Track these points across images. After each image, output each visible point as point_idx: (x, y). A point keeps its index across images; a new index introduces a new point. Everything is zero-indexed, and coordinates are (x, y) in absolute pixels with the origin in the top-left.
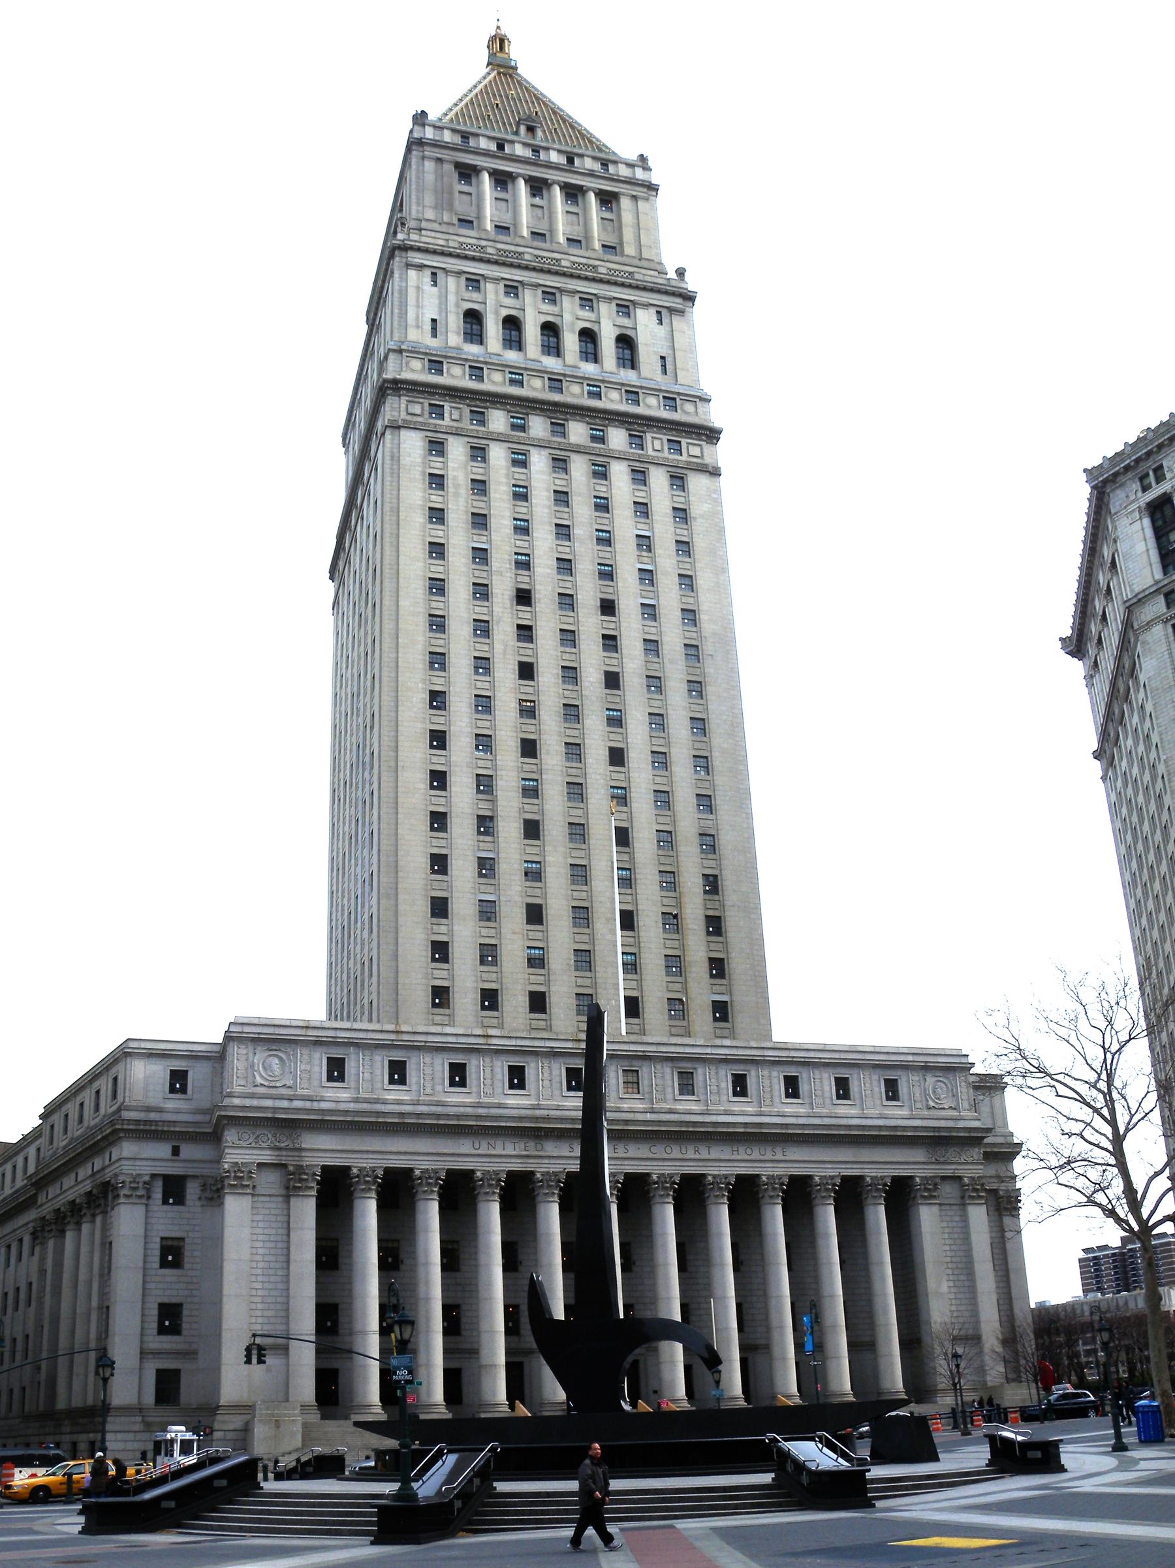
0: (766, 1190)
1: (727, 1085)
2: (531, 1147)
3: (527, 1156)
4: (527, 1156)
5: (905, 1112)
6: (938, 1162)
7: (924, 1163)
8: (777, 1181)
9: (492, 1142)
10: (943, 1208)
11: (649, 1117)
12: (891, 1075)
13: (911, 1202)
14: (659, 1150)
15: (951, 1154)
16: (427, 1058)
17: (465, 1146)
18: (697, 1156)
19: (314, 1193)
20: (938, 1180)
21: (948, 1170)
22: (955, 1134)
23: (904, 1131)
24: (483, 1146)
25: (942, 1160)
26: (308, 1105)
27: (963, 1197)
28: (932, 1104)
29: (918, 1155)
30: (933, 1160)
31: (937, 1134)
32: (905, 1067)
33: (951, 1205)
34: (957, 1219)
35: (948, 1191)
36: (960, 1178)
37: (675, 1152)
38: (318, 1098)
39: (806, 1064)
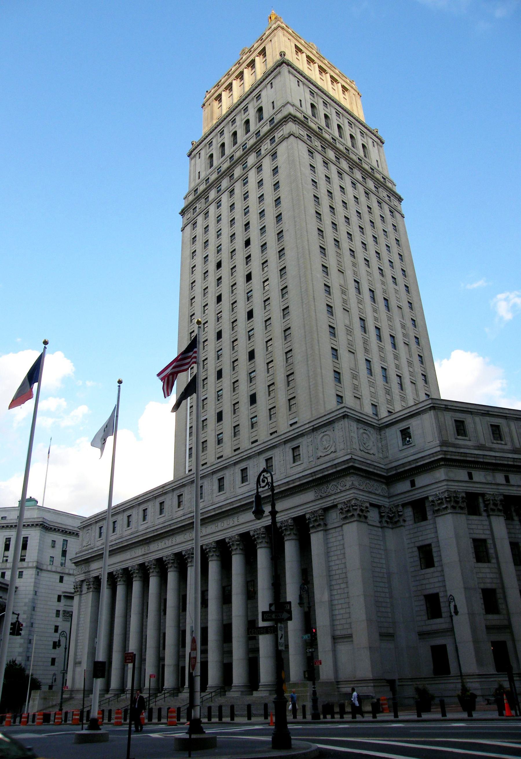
6: (322, 498)
7: (312, 501)
15: (331, 488)
21: (328, 503)
22: (326, 473)
23: (294, 483)
25: (324, 495)
29: (309, 496)
30: (319, 497)
31: (314, 477)
33: (335, 528)
35: (334, 517)
36: (335, 506)
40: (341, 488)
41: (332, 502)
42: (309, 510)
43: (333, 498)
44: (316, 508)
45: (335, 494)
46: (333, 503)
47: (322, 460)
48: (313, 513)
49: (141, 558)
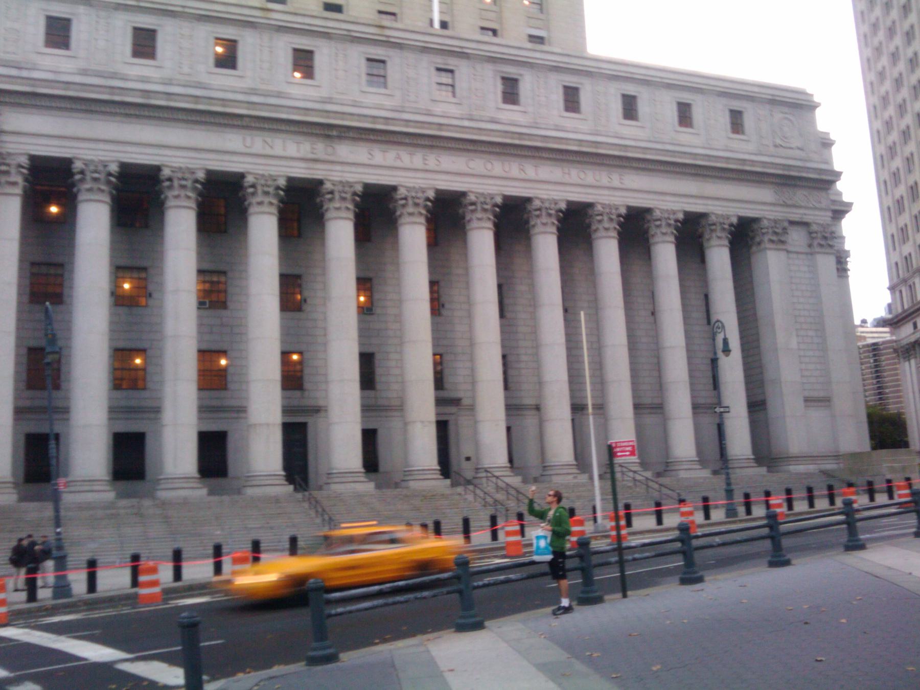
0: (600, 221)
1: (558, 98)
2: (320, 148)
3: (316, 161)
4: (316, 161)
5: (751, 147)
8: (614, 211)
9: (269, 140)
10: (791, 255)
11: (466, 123)
12: (737, 105)
13: (754, 249)
14: (478, 164)
15: (800, 196)
16: (185, 27)
17: (233, 140)
18: (523, 176)
19: (18, 190)
20: (786, 224)
24: (258, 142)
25: (789, 202)
26: (14, 72)
27: (810, 246)
28: (778, 141)
29: (765, 194)
30: (782, 203)
32: (750, 98)
34: (806, 269)
35: (797, 238)
36: (806, 224)
37: (497, 167)
38: (29, 66)
39: (646, 82)
40: (815, 204)
41: (799, 216)
42: (771, 215)
43: (801, 211)
44: (779, 216)
45: (806, 208)
46: (801, 218)
47: (782, 152)
48: (775, 221)
49: (303, 165)
